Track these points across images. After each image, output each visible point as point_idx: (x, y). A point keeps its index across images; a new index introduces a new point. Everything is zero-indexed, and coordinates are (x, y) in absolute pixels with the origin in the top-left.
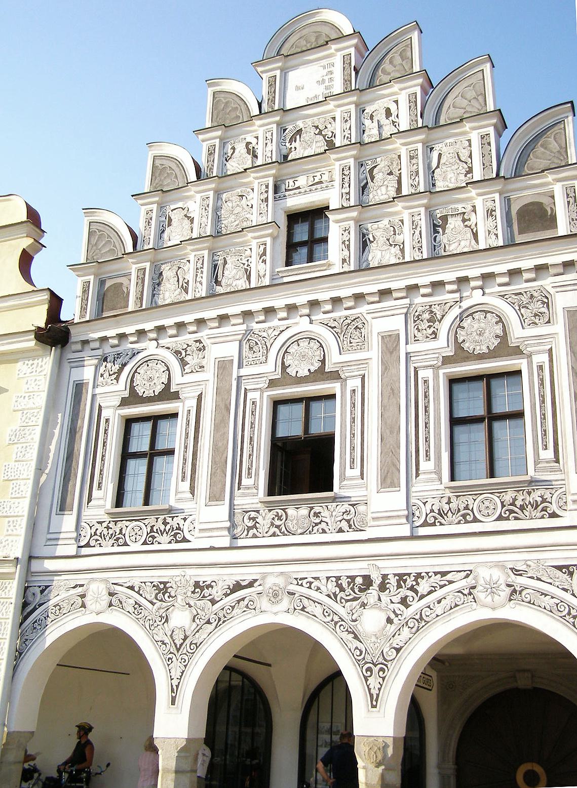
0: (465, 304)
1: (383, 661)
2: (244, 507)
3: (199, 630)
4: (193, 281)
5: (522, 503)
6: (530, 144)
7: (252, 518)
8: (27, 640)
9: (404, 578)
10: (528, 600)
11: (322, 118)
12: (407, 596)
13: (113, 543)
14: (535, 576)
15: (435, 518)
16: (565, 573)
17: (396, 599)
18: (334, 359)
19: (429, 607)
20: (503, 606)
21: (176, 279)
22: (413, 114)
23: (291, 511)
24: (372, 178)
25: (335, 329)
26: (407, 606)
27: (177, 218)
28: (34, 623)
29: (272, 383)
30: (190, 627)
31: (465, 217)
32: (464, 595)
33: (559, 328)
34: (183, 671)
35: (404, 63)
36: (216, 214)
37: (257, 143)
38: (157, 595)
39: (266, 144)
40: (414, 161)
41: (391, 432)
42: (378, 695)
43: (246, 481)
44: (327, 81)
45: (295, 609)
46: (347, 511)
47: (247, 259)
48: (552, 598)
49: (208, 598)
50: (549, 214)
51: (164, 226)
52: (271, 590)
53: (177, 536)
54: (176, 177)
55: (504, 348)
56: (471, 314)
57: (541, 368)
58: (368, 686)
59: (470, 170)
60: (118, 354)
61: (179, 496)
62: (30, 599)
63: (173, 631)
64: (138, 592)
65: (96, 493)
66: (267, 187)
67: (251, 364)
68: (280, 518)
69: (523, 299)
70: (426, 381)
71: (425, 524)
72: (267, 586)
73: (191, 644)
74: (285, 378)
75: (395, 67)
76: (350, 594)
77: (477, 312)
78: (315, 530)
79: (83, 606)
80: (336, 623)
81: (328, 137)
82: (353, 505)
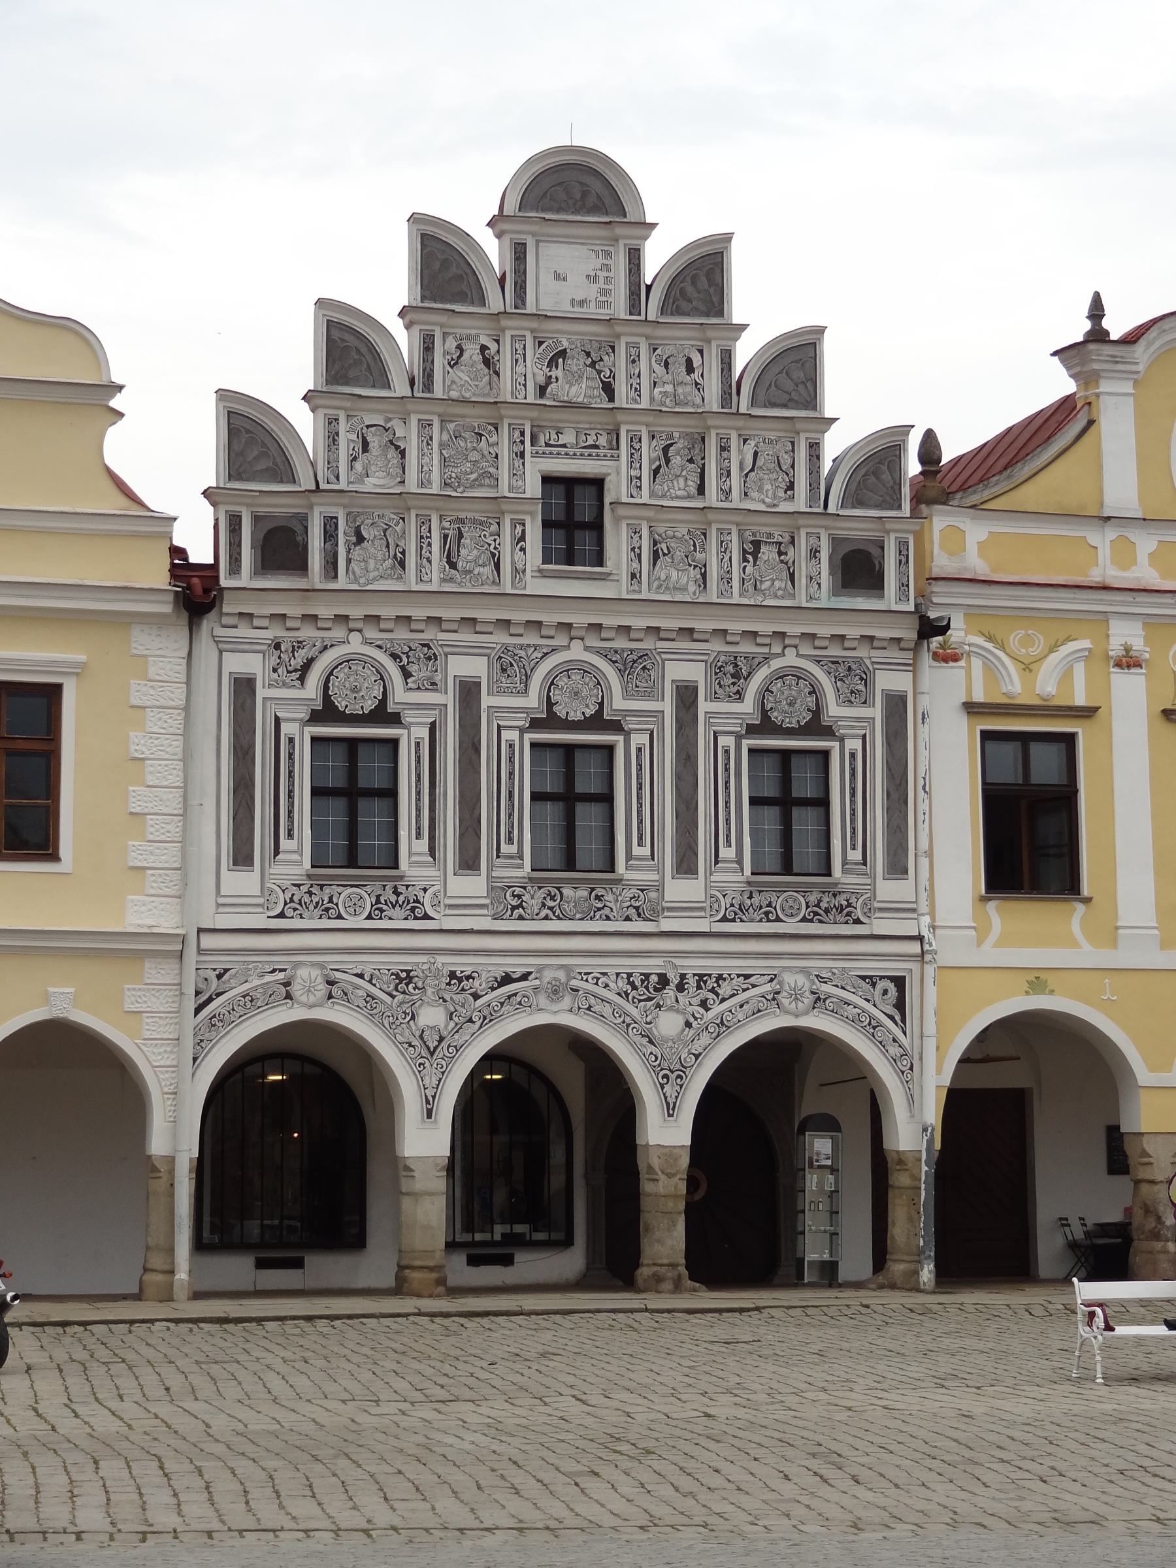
0: (776, 664)
1: (681, 1068)
2: (504, 880)
3: (459, 1029)
4: (416, 556)
5: (826, 905)
6: (861, 466)
7: (517, 896)
8: (202, 1041)
9: (705, 979)
10: (831, 1008)
11: (596, 341)
12: (707, 999)
13: (321, 915)
14: (839, 984)
15: (736, 914)
16: (868, 983)
17: (696, 1001)
18: (618, 702)
19: (730, 1011)
20: (806, 1013)
21: (385, 543)
22: (725, 383)
23: (568, 892)
24: (668, 461)
25: (617, 665)
26: (707, 1009)
27: (377, 442)
28: (211, 1019)
29: (536, 724)
30: (448, 1027)
31: (782, 548)
32: (767, 1000)
33: (876, 712)
34: (440, 1079)
35: (712, 290)
36: (441, 453)
37: (498, 351)
38: (397, 985)
39: (517, 361)
40: (725, 454)
41: (688, 809)
42: (675, 1104)
43: (505, 848)
44: (602, 280)
45: (579, 1008)
46: (634, 897)
47: (493, 538)
48: (855, 1007)
49: (468, 992)
50: (877, 569)
51: (356, 449)
52: (549, 986)
53: (415, 910)
54: (369, 367)
55: (817, 726)
56: (782, 677)
57: (853, 755)
58: (664, 1094)
59: (791, 486)
60: (299, 642)
61: (414, 859)
62: (201, 986)
63: (423, 1031)
64: (370, 981)
65: (284, 843)
66: (522, 434)
67: (504, 692)
68: (553, 898)
69: (840, 670)
70: (727, 752)
71: (724, 919)
72: (546, 980)
73: (449, 1046)
74: (550, 721)
75: (699, 293)
76: (644, 994)
77: (788, 675)
78: (597, 917)
79: (289, 996)
80: (628, 1025)
81: (604, 376)
82: (642, 890)
